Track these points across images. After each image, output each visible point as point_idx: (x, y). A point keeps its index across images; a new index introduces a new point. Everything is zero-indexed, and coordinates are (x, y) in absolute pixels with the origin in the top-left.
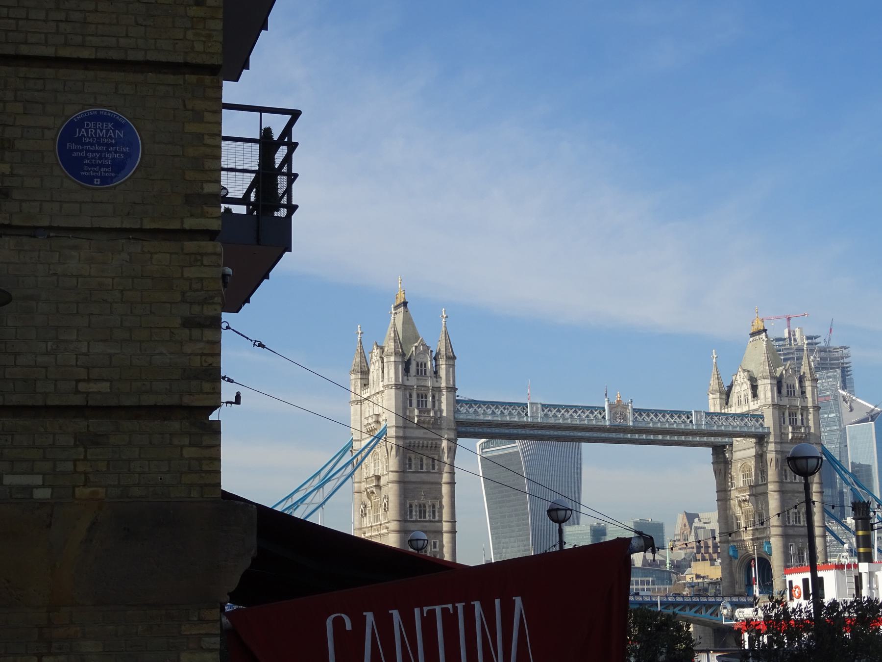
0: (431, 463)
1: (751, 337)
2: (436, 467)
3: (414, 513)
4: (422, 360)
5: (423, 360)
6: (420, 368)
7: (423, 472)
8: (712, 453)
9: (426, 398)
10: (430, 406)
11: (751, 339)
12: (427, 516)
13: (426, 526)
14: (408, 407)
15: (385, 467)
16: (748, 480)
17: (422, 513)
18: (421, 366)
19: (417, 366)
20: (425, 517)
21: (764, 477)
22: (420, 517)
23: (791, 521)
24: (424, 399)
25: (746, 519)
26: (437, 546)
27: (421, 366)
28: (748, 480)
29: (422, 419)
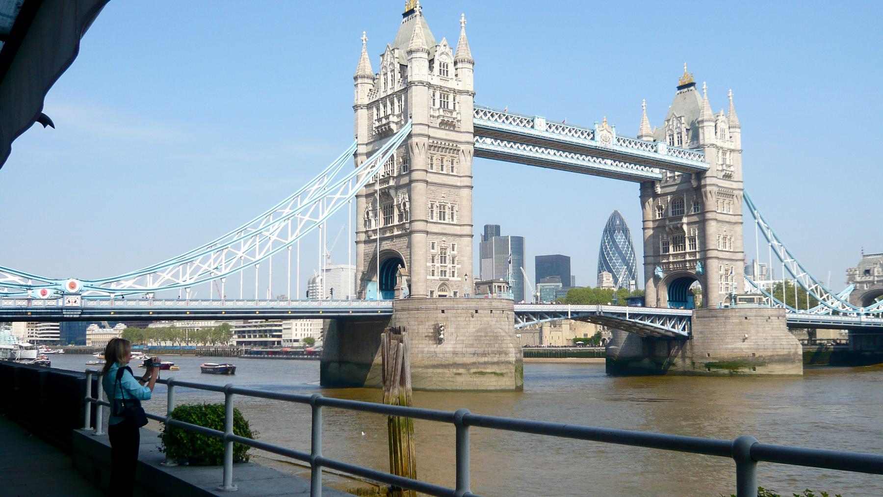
0: (451, 166)
1: (679, 90)
2: (455, 170)
3: (435, 214)
4: (444, 61)
5: (445, 61)
6: (442, 68)
7: (444, 174)
8: (639, 188)
9: (447, 99)
10: (451, 107)
11: (678, 92)
12: (447, 217)
13: (445, 229)
14: (432, 106)
15: (402, 168)
16: (681, 210)
17: (442, 215)
18: (444, 67)
19: (440, 66)
20: (444, 220)
21: (698, 208)
22: (440, 219)
23: (720, 246)
24: (446, 100)
25: (690, 242)
26: (455, 249)
27: (444, 67)
28: (681, 210)
29: (446, 120)
